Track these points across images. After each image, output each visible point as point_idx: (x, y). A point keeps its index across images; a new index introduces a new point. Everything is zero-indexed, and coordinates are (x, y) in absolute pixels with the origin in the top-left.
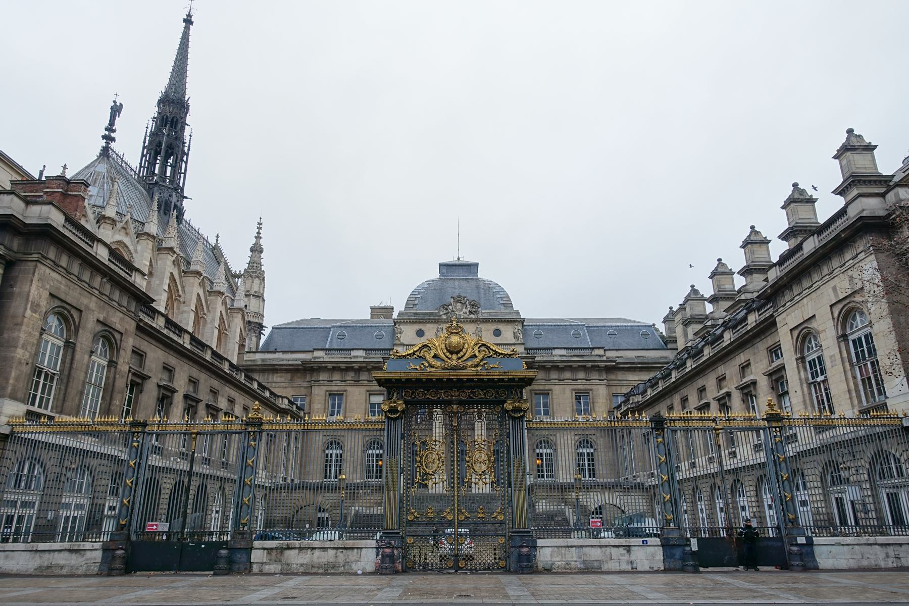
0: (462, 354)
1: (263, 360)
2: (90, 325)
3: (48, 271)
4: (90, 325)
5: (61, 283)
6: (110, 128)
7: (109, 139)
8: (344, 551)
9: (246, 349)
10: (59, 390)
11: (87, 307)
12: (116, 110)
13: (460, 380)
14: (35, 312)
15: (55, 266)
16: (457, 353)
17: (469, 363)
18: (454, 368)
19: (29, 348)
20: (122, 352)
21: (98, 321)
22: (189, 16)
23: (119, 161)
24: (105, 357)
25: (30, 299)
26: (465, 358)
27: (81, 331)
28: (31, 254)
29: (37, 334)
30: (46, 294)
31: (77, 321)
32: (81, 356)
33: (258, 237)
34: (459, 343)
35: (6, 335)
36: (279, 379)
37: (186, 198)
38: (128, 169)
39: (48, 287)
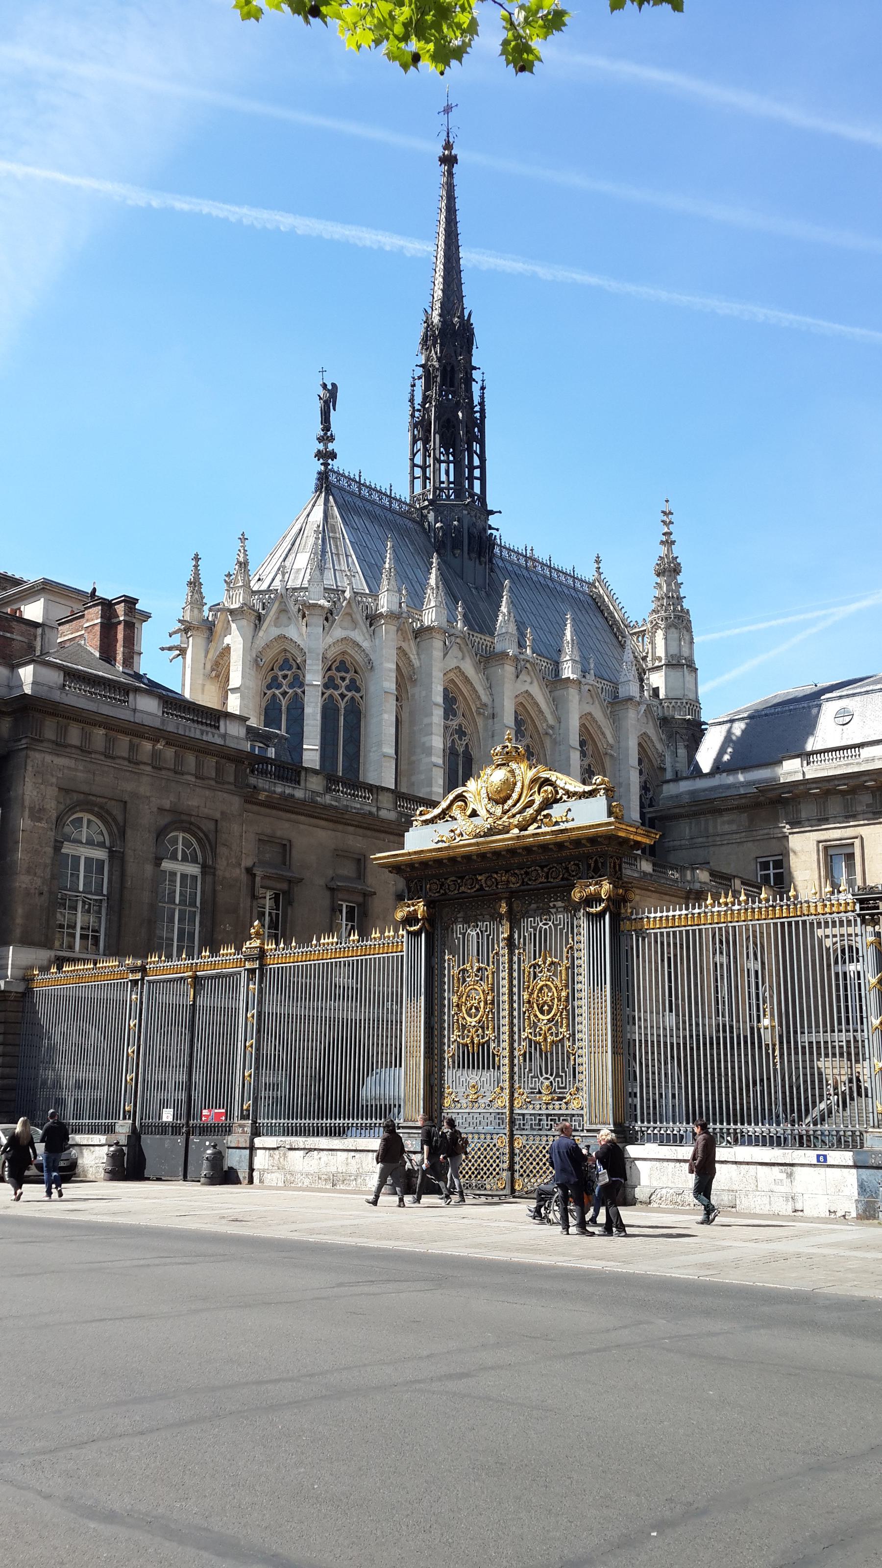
0: (510, 802)
1: (692, 793)
2: (146, 817)
3: (48, 758)
4: (146, 817)
5: (76, 770)
6: (326, 437)
7: (327, 456)
8: (357, 1155)
9: (669, 775)
10: (109, 921)
11: (135, 795)
12: (330, 399)
13: (497, 853)
14: (40, 820)
15: (60, 746)
16: (504, 801)
17: (515, 821)
18: (491, 832)
19: (39, 872)
20: (222, 850)
21: (161, 810)
22: (448, 146)
23: (355, 487)
24: (195, 861)
25: (27, 803)
26: (515, 810)
27: (129, 832)
28: (20, 740)
29: (49, 850)
30: (51, 792)
31: (120, 818)
32: (139, 869)
33: (668, 543)
34: (506, 782)
35: (9, 859)
36: (727, 828)
37: (492, 512)
38: (375, 496)
39: (54, 780)
